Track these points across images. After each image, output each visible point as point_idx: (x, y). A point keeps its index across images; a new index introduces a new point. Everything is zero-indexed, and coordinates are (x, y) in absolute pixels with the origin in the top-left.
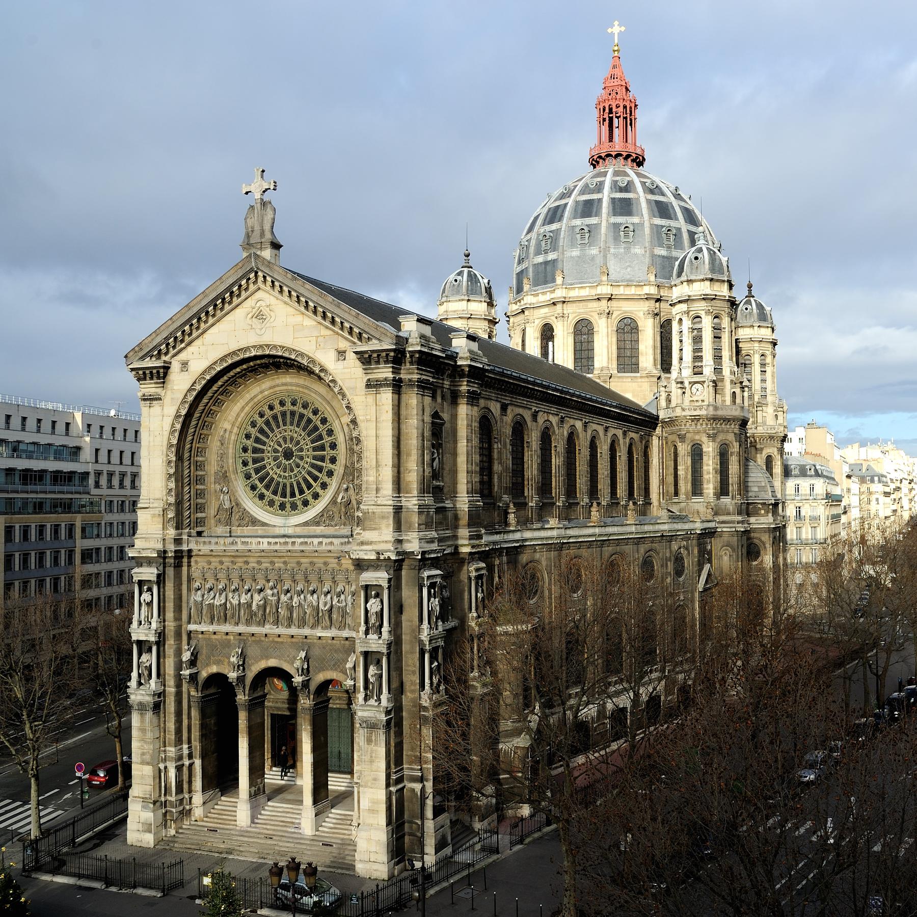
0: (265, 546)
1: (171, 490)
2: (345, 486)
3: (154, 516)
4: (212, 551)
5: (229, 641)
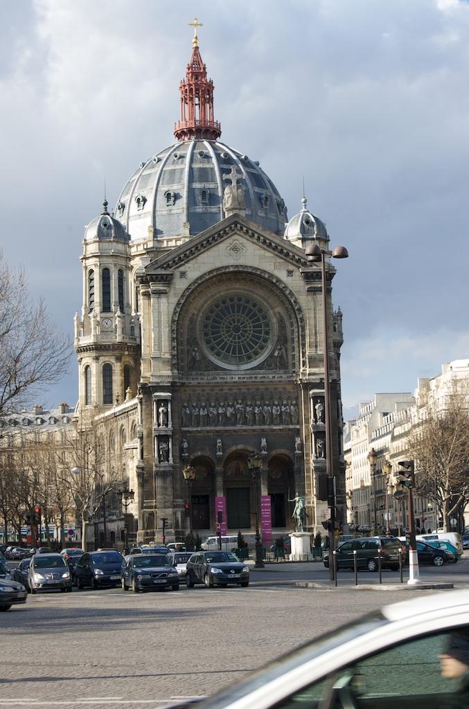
0: (237, 379)
1: (174, 347)
2: (279, 347)
3: (164, 362)
4: (199, 383)
5: (209, 436)
